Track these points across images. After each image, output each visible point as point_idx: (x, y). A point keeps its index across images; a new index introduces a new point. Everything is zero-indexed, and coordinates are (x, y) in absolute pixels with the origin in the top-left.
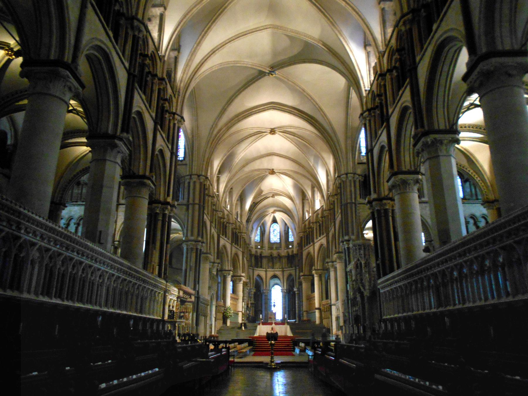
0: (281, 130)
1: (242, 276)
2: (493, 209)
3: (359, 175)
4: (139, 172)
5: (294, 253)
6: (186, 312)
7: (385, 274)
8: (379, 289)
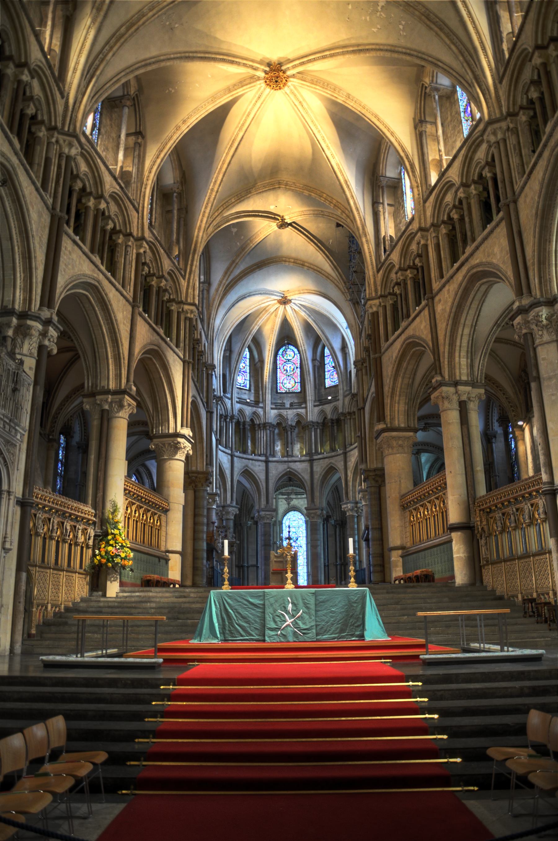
1: (183, 436)
5: (340, 411)
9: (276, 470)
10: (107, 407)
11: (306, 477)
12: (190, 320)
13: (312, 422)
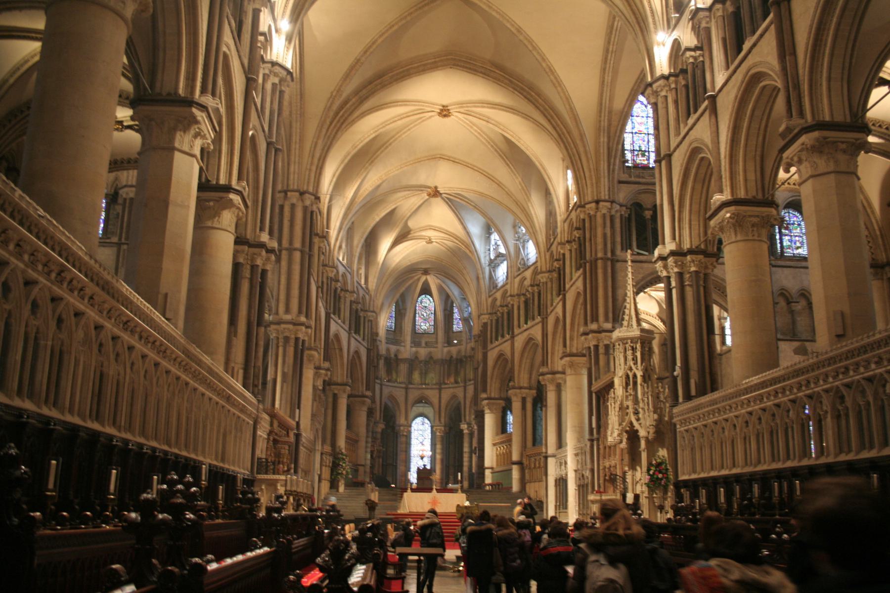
0: (462, 110)
2: (882, 279)
3: (621, 206)
4: (218, 179)
6: (279, 463)
7: (688, 397)
8: (675, 425)
9: (414, 394)
10: (336, 392)
11: (435, 401)
12: (371, 321)
13: (442, 360)
